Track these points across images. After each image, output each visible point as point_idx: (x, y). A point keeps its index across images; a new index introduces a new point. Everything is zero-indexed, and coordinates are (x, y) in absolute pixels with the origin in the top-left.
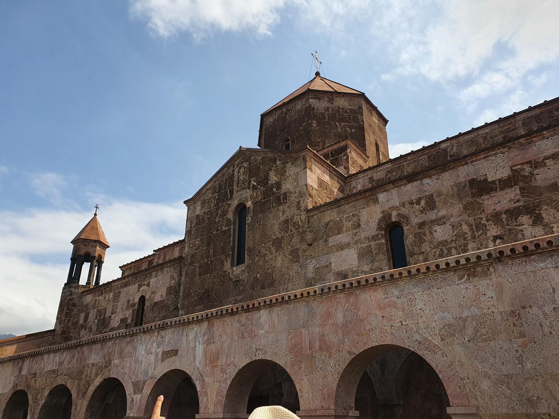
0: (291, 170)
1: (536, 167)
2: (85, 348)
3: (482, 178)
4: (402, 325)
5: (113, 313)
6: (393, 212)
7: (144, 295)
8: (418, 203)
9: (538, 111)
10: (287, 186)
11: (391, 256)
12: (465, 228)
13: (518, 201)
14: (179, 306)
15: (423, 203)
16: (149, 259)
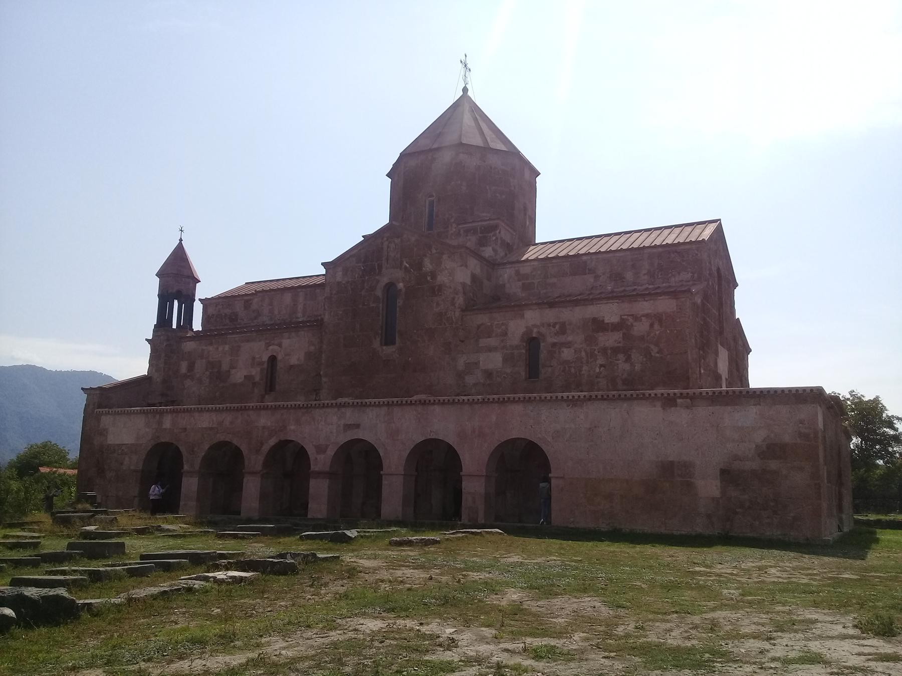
0: (448, 263)
1: (636, 321)
2: (251, 412)
3: (601, 319)
4: (532, 427)
5: (232, 367)
6: (536, 329)
7: (275, 354)
8: (554, 327)
9: (660, 250)
10: (442, 278)
11: (528, 363)
12: (583, 354)
13: (620, 343)
14: (322, 373)
15: (557, 327)
16: (246, 298)
